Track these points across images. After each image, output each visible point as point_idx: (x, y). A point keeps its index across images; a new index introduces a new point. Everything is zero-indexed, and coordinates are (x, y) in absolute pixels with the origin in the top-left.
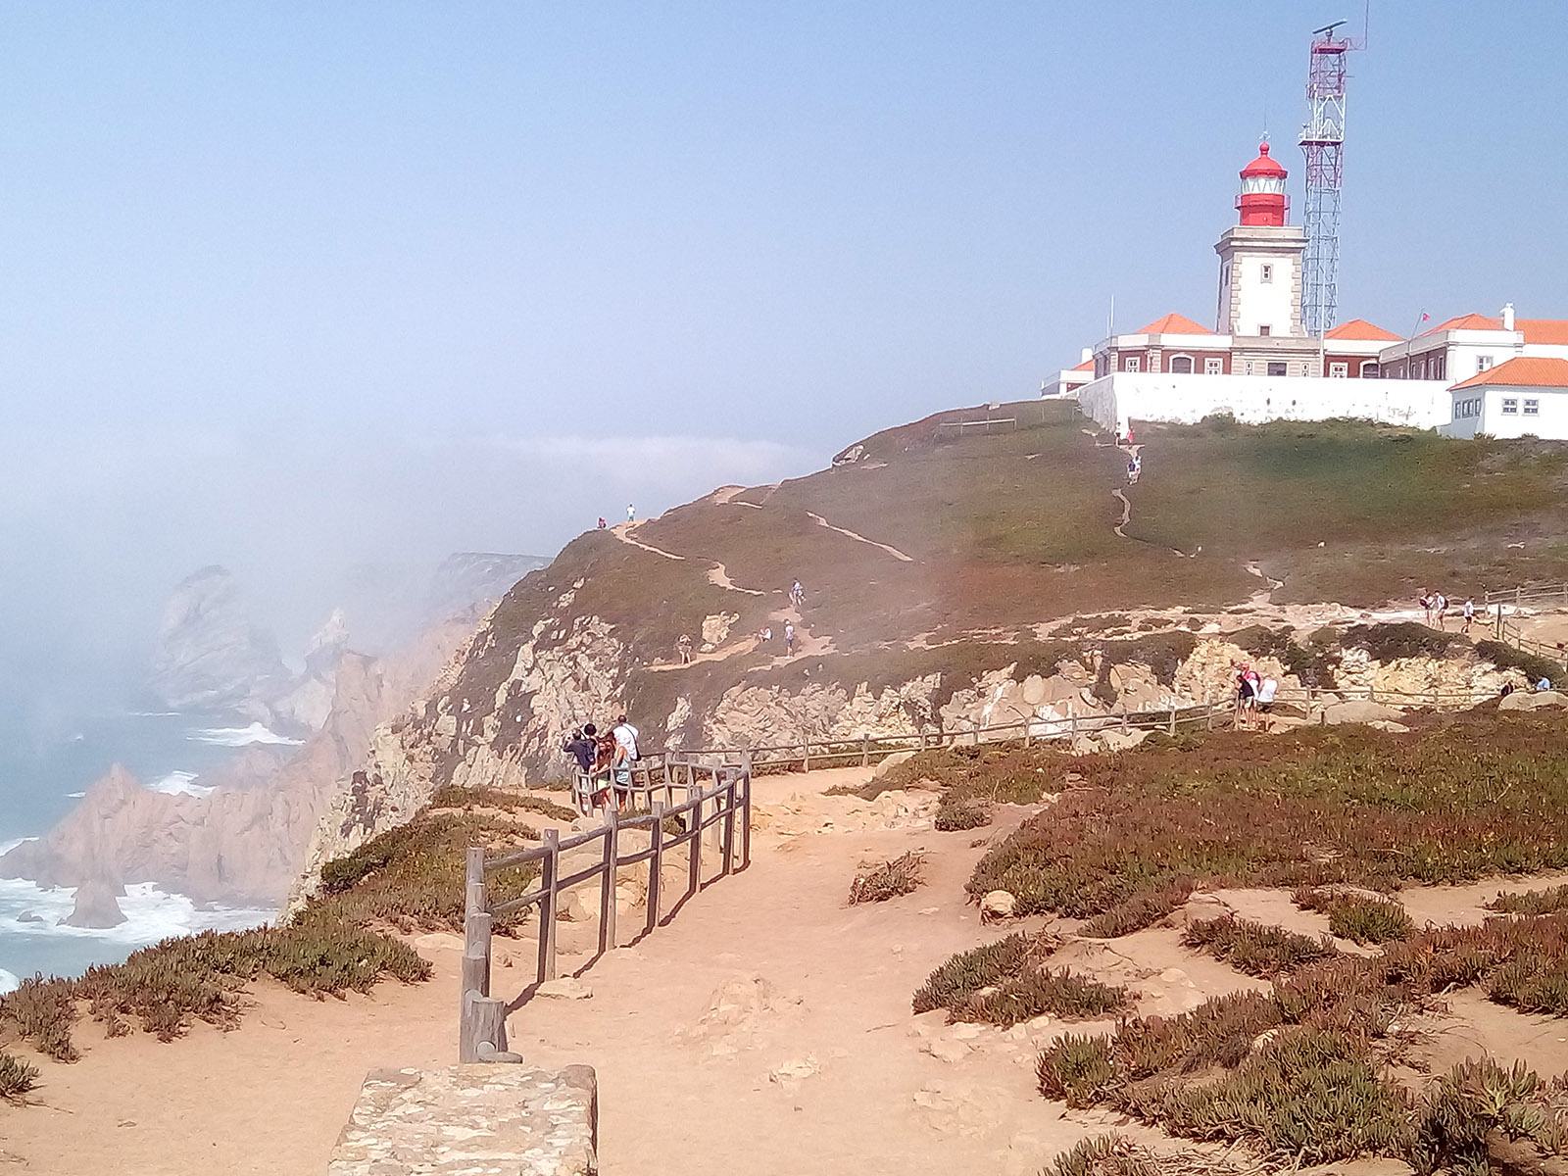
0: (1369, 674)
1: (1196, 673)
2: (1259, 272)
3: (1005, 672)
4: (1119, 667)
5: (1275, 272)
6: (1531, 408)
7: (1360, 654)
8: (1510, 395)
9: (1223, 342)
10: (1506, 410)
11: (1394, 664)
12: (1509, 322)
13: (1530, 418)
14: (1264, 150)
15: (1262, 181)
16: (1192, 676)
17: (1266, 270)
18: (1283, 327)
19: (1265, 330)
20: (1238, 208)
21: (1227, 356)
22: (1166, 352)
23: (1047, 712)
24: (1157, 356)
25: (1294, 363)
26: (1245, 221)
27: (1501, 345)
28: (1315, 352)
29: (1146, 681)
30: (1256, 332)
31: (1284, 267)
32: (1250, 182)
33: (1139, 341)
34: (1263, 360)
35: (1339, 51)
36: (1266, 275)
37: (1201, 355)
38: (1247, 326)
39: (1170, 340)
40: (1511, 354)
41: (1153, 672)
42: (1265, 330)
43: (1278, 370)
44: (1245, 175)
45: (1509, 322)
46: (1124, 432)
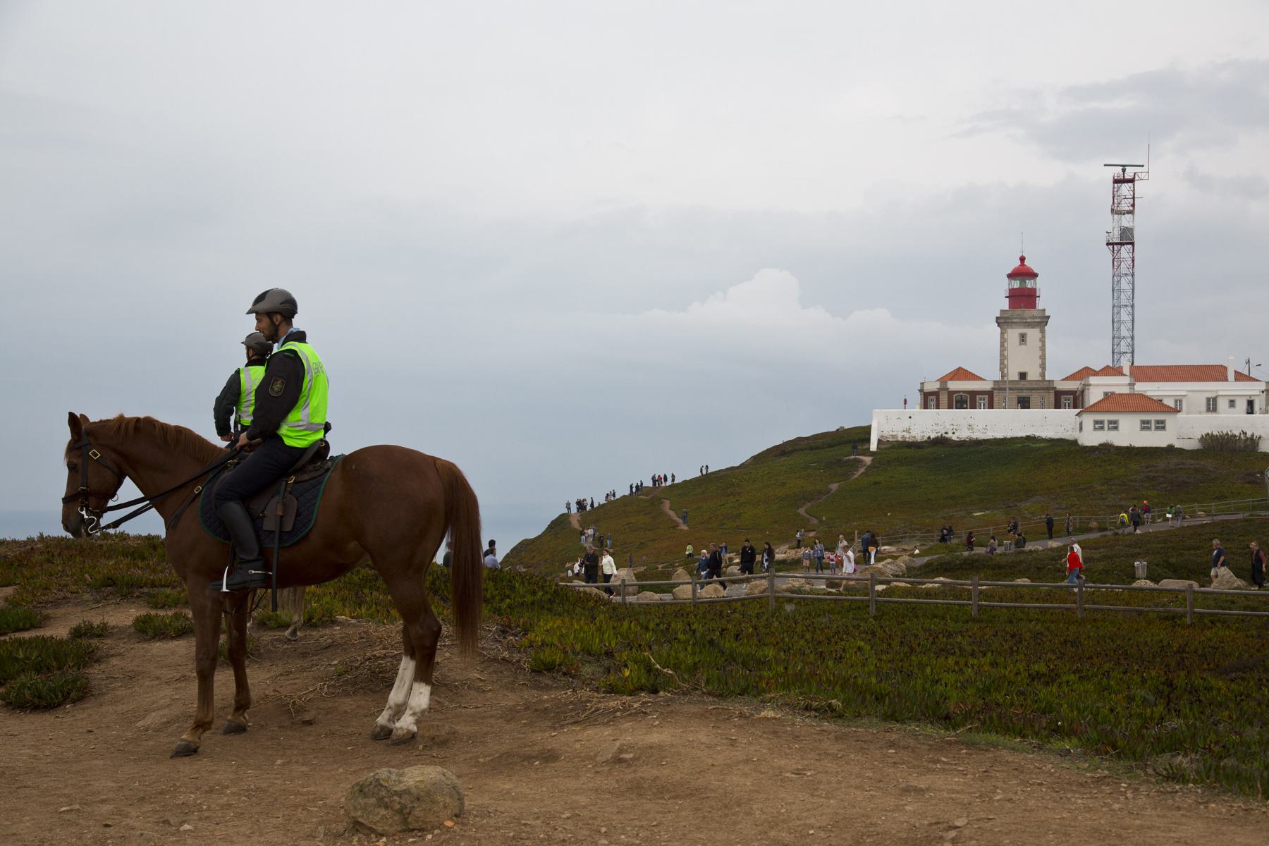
5: (1029, 339)
6: (1114, 426)
9: (987, 386)
12: (1126, 370)
13: (1113, 433)
14: (1022, 259)
17: (1023, 338)
19: (1023, 376)
21: (990, 394)
22: (951, 393)
24: (944, 398)
25: (1035, 397)
26: (1011, 306)
27: (1119, 385)
28: (1048, 389)
30: (1016, 378)
31: (1033, 334)
33: (935, 387)
34: (1014, 397)
35: (1132, 181)
37: (973, 394)
39: (954, 385)
40: (1126, 390)
43: (1024, 403)
44: (1010, 276)
45: (1126, 370)
46: (873, 447)
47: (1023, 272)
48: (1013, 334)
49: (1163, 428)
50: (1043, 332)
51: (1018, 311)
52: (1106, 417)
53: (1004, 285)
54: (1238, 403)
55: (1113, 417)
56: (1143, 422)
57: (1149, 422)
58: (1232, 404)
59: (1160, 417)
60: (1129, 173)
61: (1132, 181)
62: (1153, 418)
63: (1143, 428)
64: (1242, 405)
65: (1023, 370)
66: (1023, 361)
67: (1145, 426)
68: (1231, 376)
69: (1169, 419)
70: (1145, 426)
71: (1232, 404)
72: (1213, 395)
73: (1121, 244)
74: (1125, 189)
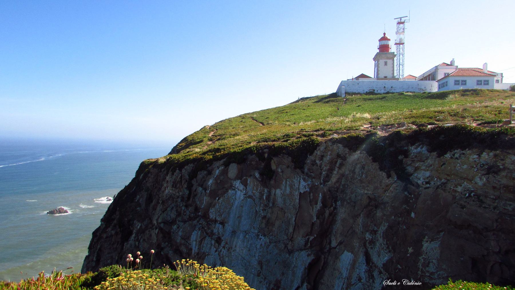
0: (430, 161)
1: (318, 162)
2: (384, 64)
3: (222, 162)
4: (275, 159)
5: (388, 64)
7: (422, 148)
11: (448, 156)
14: (385, 34)
16: (314, 163)
17: (386, 64)
18: (389, 75)
23: (237, 184)
29: (288, 167)
30: (383, 77)
31: (389, 62)
35: (403, 23)
41: (292, 161)
42: (386, 77)
44: (380, 40)
47: (384, 38)
48: (382, 62)
50: (393, 60)
53: (377, 44)
60: (402, 21)
61: (403, 23)
65: (385, 76)
66: (385, 71)
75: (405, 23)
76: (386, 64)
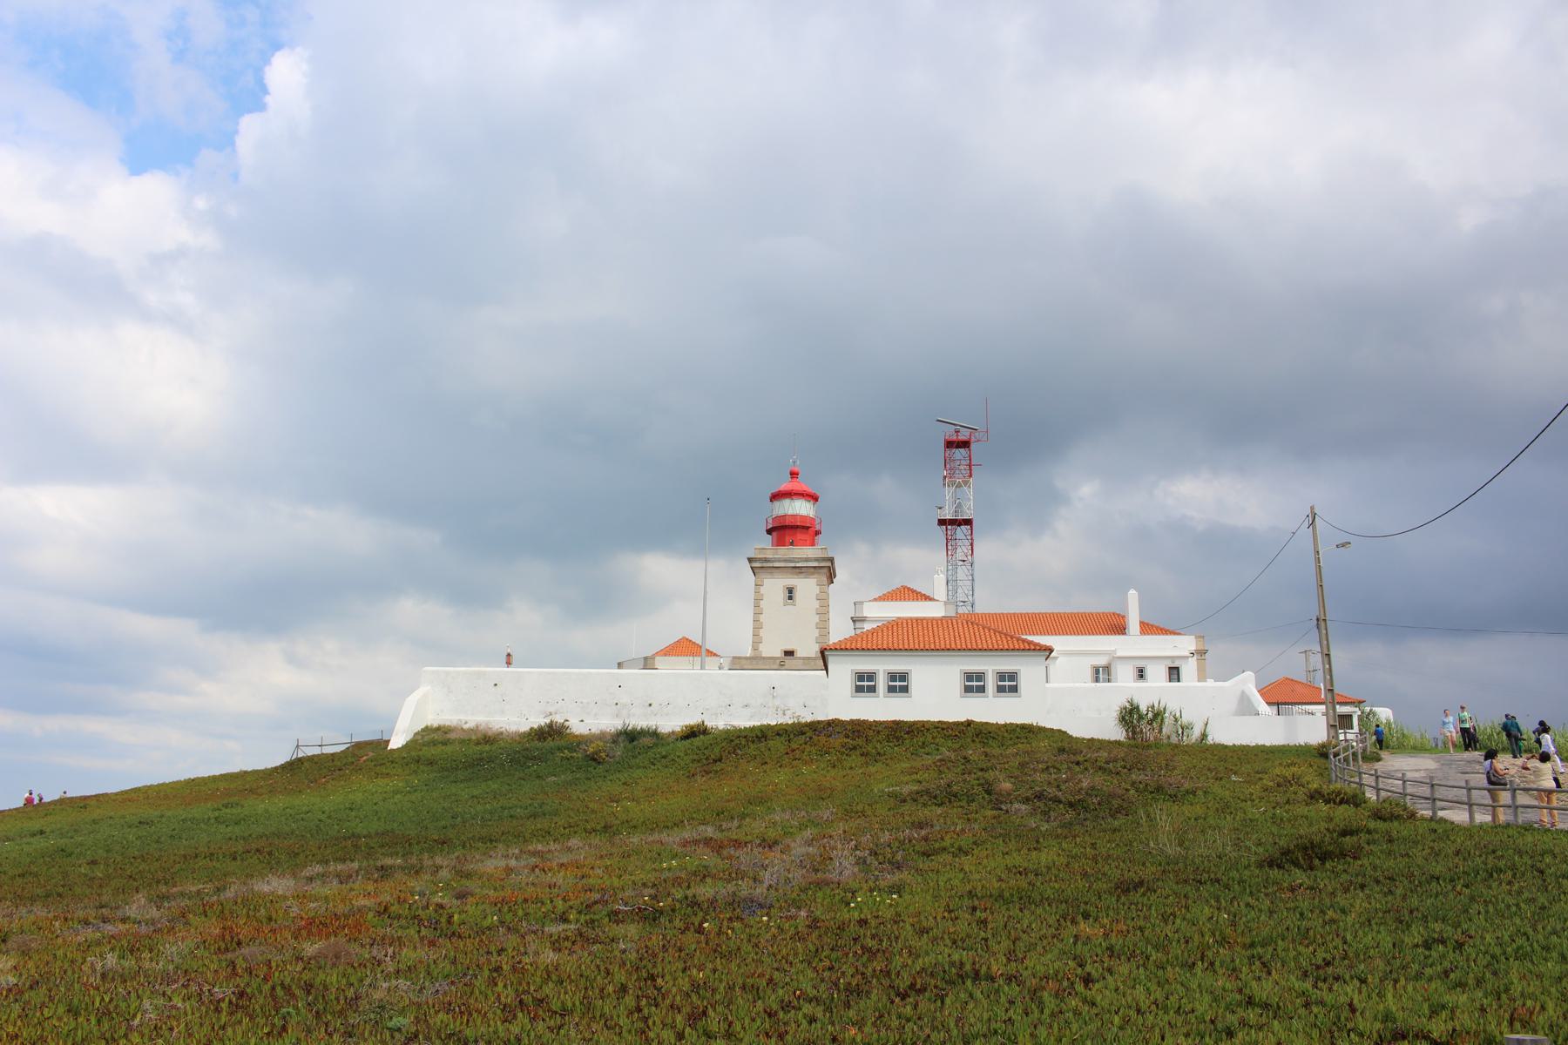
2: (781, 595)
5: (798, 594)
8: (866, 664)
10: (859, 689)
15: (786, 502)
17: (790, 590)
20: (769, 532)
31: (807, 587)
32: (777, 504)
35: (965, 444)
36: (790, 598)
38: (772, 649)
42: (789, 653)
48: (774, 586)
49: (1014, 689)
51: (785, 552)
52: (882, 666)
54: (1149, 672)
55: (897, 664)
56: (969, 676)
57: (980, 676)
58: (1141, 674)
59: (1007, 664)
61: (965, 444)
62: (990, 666)
63: (968, 689)
64: (1157, 674)
65: (789, 648)
67: (973, 684)
68: (1133, 624)
69: (1028, 670)
70: (973, 684)
71: (1141, 674)
72: (1102, 661)
73: (953, 522)
74: (960, 453)
75: (973, 446)
76: (790, 590)
